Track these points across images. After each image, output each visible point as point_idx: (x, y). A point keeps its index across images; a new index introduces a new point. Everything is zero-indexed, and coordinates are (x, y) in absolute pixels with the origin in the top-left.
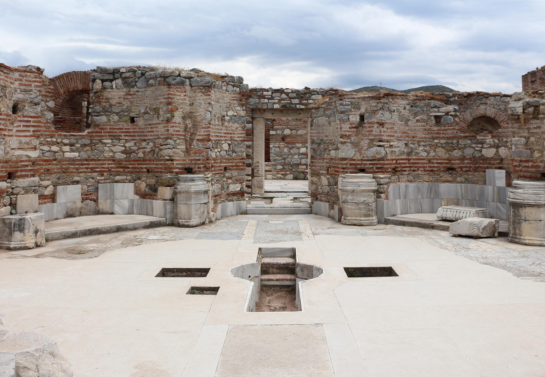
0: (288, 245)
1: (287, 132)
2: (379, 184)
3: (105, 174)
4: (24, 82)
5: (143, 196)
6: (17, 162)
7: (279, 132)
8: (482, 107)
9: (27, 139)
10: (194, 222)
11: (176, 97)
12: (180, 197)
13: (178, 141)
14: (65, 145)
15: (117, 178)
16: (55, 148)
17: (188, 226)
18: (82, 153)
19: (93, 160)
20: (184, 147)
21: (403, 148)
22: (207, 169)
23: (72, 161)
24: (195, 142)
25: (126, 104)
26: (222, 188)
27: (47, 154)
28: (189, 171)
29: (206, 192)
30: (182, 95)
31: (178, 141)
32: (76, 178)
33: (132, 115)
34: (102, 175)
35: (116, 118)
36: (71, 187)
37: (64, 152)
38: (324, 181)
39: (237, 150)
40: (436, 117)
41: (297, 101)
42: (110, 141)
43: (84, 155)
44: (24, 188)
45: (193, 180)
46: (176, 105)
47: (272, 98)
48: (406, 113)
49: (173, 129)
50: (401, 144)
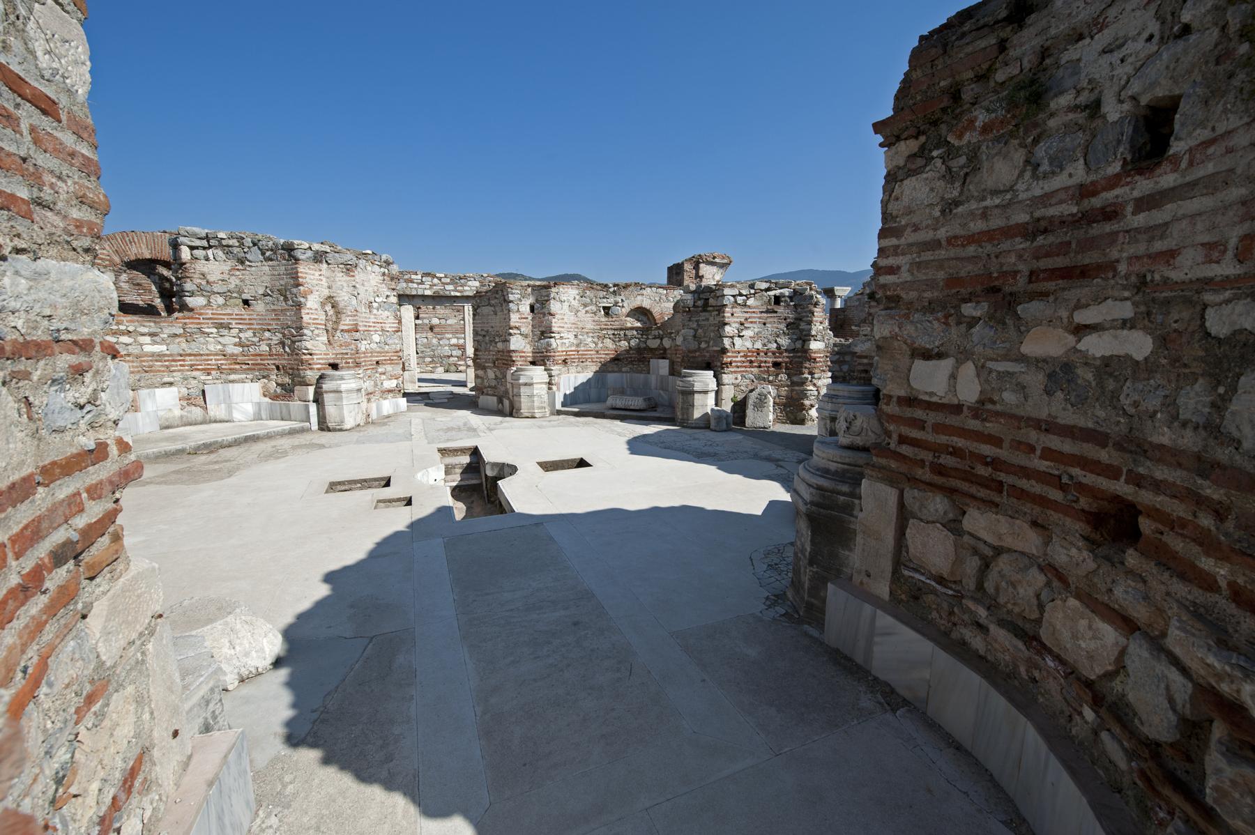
0: (469, 443)
1: (435, 321)
2: (550, 376)
3: (213, 372)
5: (275, 397)
7: (426, 321)
8: (639, 298)
10: (347, 426)
12: (327, 398)
13: (316, 332)
15: (232, 377)
17: (341, 430)
18: (171, 347)
19: (190, 355)
20: (325, 339)
21: (572, 339)
22: (358, 365)
23: (160, 356)
24: (338, 333)
25: (234, 282)
26: (376, 385)
28: (334, 366)
29: (359, 390)
30: (317, 273)
32: (166, 379)
33: (245, 296)
34: (209, 374)
35: (221, 300)
36: (160, 392)
37: (141, 345)
38: (491, 374)
39: (390, 342)
40: (604, 308)
41: (451, 287)
42: (214, 330)
43: (175, 349)
45: (342, 379)
47: (422, 283)
48: (575, 303)
50: (571, 336)
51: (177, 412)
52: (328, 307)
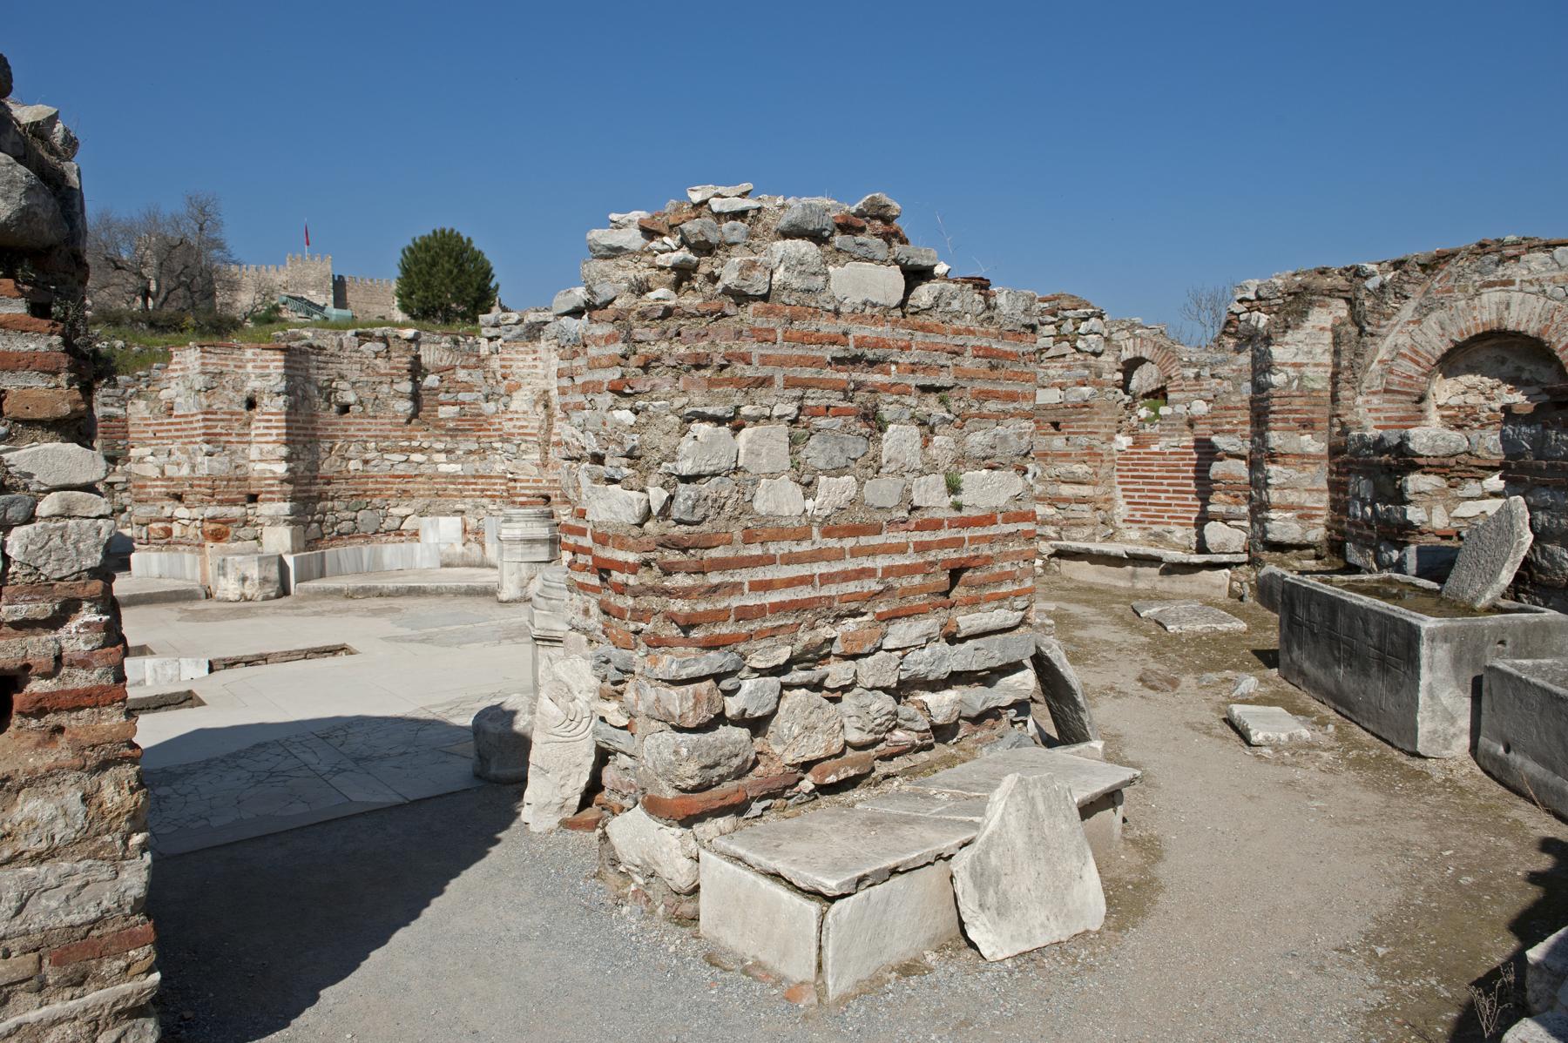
4: (259, 363)
6: (260, 479)
9: (270, 447)
11: (515, 364)
14: (439, 452)
16: (416, 457)
19: (482, 477)
20: (536, 456)
27: (402, 466)
30: (530, 358)
31: (523, 447)
32: (459, 506)
44: (271, 518)
46: (517, 378)
49: (511, 424)
51: (459, 548)
52: (540, 408)
